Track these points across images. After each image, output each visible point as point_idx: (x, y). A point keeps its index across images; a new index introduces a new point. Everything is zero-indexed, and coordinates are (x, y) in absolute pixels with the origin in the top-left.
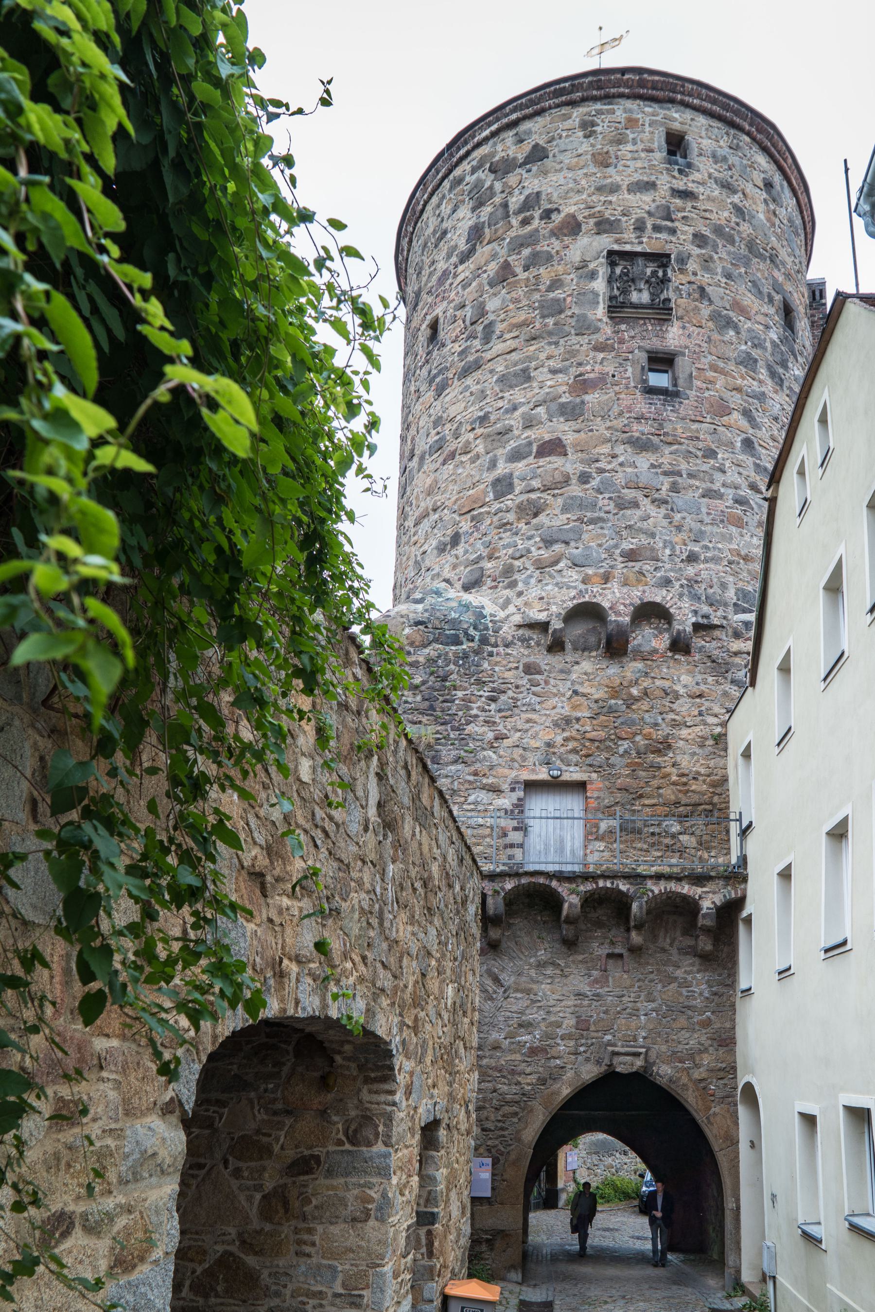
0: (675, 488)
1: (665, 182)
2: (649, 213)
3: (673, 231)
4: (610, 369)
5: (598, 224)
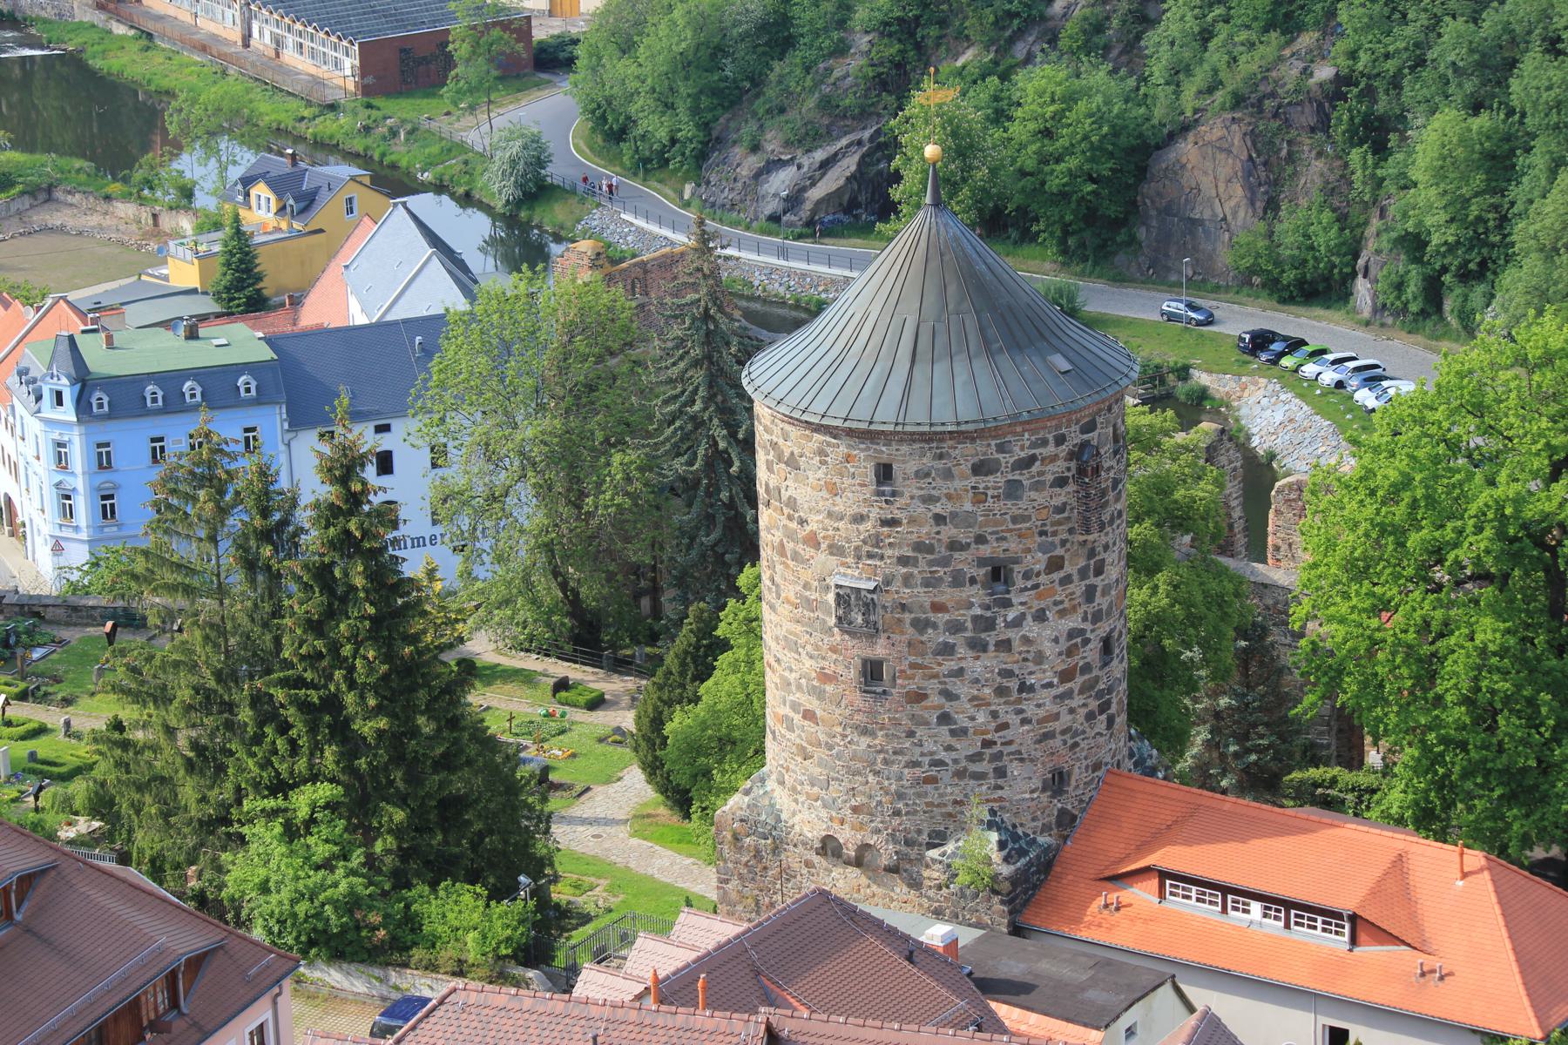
0: (886, 762)
1: (875, 513)
2: (864, 542)
3: (882, 558)
4: (840, 669)
5: (830, 547)
